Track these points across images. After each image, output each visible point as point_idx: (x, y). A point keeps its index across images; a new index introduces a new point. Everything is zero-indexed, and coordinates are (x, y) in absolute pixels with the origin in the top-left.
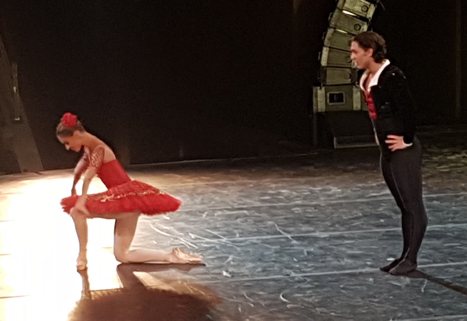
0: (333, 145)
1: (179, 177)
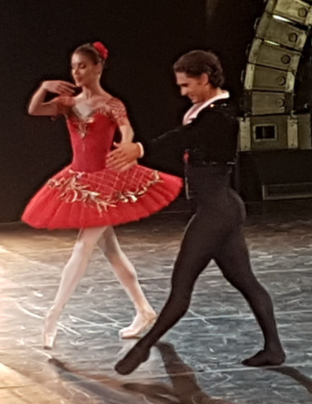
0: (262, 197)
1: (55, 239)
